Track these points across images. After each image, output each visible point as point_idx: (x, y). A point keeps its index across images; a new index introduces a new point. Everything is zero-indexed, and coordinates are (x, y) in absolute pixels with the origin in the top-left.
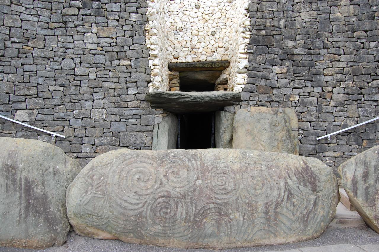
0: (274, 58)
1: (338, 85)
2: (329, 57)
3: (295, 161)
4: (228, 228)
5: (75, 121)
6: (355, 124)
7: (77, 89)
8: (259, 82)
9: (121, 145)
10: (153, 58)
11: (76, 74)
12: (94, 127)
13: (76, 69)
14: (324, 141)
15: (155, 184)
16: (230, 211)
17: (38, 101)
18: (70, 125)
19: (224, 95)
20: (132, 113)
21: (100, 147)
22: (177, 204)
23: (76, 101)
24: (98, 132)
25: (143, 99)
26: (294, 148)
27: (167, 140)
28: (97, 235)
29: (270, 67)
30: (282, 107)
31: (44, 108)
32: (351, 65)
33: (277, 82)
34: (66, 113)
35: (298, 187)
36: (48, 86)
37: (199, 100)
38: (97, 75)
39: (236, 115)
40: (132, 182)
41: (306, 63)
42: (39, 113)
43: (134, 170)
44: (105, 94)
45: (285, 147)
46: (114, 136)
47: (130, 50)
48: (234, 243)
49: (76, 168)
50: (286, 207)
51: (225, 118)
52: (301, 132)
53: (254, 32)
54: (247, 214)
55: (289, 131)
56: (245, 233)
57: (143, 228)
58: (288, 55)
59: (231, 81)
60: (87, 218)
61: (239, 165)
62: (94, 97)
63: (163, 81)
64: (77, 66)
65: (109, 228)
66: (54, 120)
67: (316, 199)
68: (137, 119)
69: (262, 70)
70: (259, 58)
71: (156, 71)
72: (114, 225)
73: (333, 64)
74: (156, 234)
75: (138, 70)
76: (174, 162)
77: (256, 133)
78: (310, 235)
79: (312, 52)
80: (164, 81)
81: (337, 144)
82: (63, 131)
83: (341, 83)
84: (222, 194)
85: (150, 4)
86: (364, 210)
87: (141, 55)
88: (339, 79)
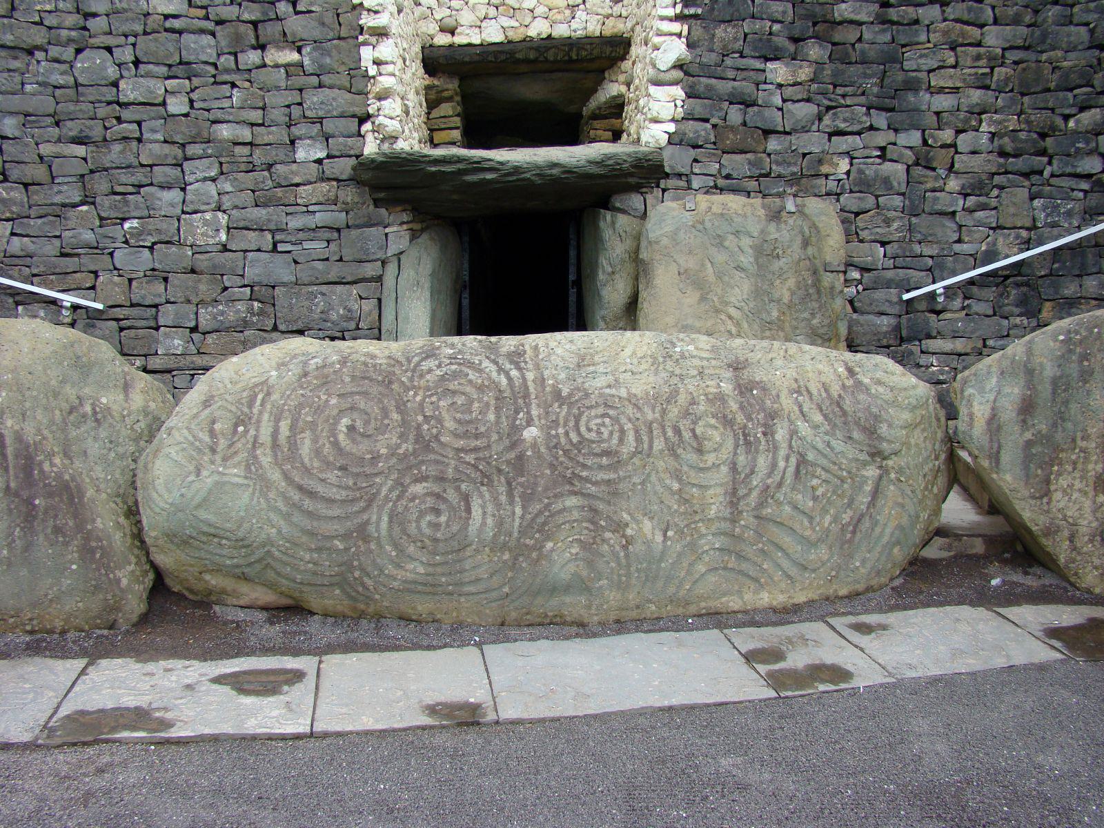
0: (770, 34)
1: (974, 123)
2: (946, 33)
3: (823, 365)
4: (619, 564)
5: (131, 254)
6: (1022, 251)
7: (131, 150)
8: (722, 114)
9: (282, 327)
10: (373, 40)
11: (126, 100)
12: (193, 271)
13: (122, 84)
14: (923, 306)
15: (399, 441)
16: (625, 516)
17: (8, 193)
18: (116, 269)
19: (610, 158)
20: (311, 221)
21: (214, 336)
22: (466, 498)
23: (131, 189)
24: (204, 287)
25: (344, 177)
26: (833, 325)
27: (428, 308)
28: (234, 593)
29: (758, 64)
30: (795, 196)
31: (28, 217)
32: (1016, 59)
33: (780, 113)
34: (100, 231)
35: (829, 442)
36: (37, 144)
37: (528, 175)
38: (191, 102)
39: (650, 224)
40: (332, 439)
42: (13, 234)
43: (333, 401)
44: (221, 164)
45: (803, 324)
46: (256, 300)
47: (297, 13)
48: (638, 607)
49: (160, 400)
50: (789, 503)
51: (614, 233)
52: (856, 275)
54: (677, 525)
55: (815, 272)
56: (669, 579)
57: (369, 569)
58: (815, 24)
59: (632, 107)
60: (205, 547)
61: (651, 379)
62: (187, 173)
63: (407, 113)
64: (125, 73)
65: (271, 575)
66: (63, 255)
67: (881, 477)
68: (328, 242)
69: (731, 74)
70: (723, 33)
71: (386, 82)
72: (286, 564)
73: (959, 54)
74: (407, 586)
75: (326, 79)
76: (455, 375)
77: (712, 278)
78: (859, 583)
79: (893, 14)
80: (411, 113)
81: (964, 312)
82: (93, 288)
83: (983, 116)
84: (601, 467)
86: (1017, 507)
87: (332, 30)
88: (977, 104)
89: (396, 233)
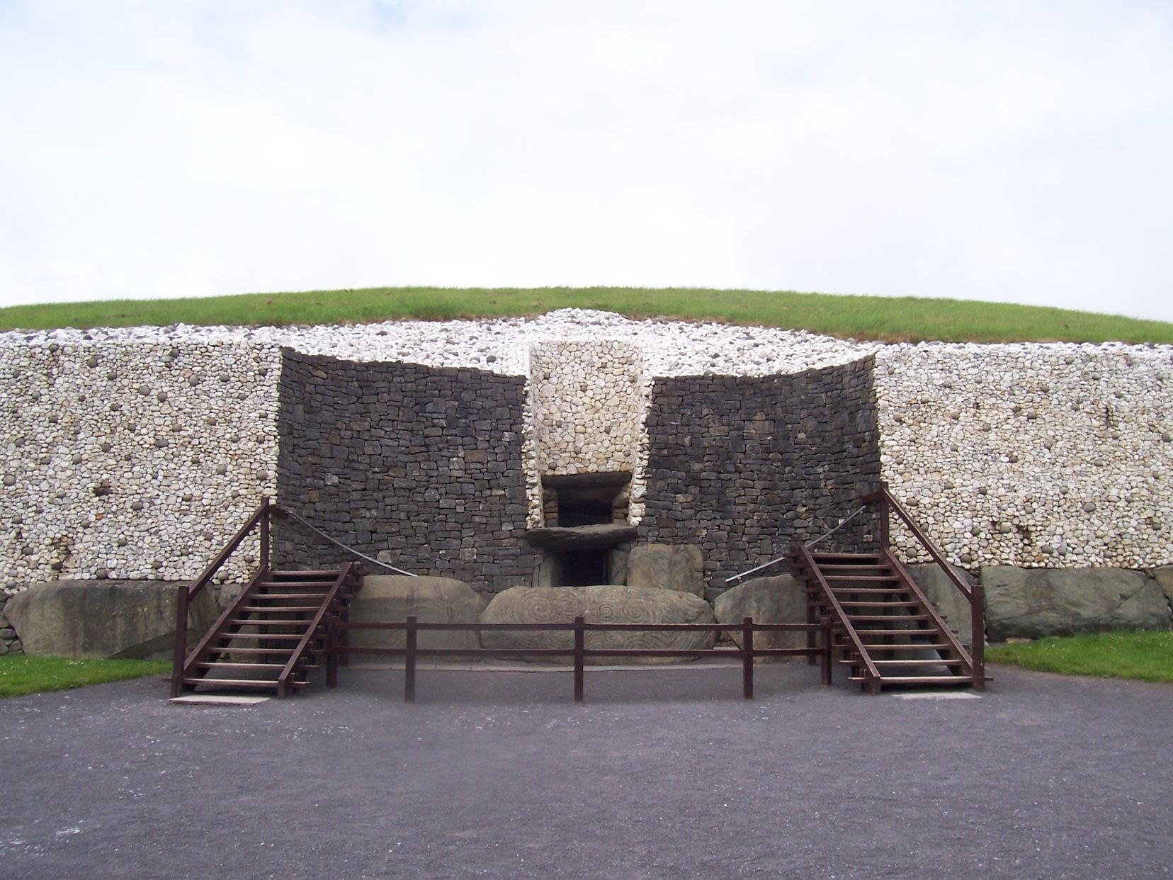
3: (673, 596)
41: (714, 490)
51: (618, 559)
53: (654, 451)
70: (660, 484)
71: (536, 502)
79: (722, 476)
85: (527, 420)
89: (538, 558)
